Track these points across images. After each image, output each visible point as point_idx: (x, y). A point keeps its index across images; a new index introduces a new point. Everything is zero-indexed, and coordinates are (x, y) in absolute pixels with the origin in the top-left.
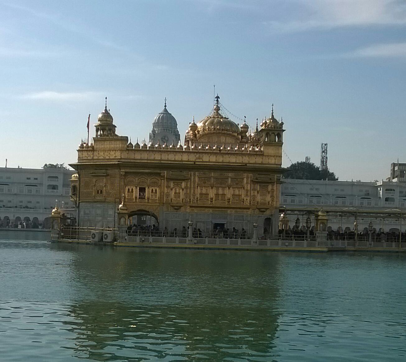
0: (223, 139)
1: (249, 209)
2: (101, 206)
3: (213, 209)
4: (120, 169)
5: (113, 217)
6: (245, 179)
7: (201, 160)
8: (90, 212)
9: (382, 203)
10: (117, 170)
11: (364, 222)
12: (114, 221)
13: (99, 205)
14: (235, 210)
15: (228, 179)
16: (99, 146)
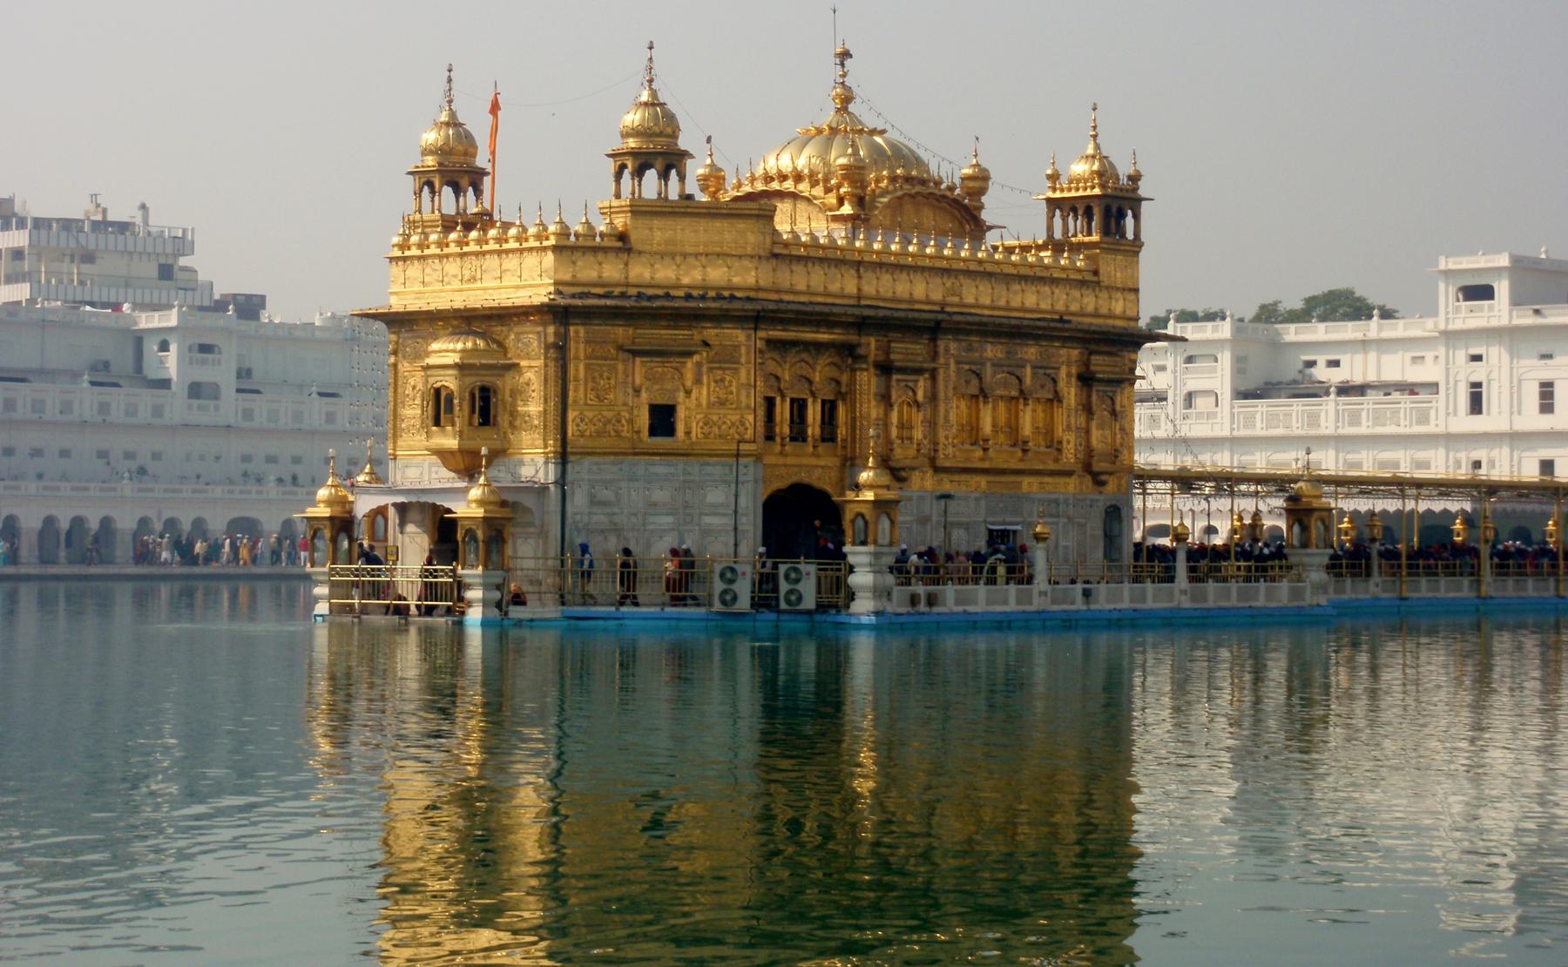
0: (928, 217)
1: (1069, 474)
2: (672, 470)
3: (991, 478)
4: (756, 329)
5: (724, 515)
6: (1063, 371)
7: (956, 299)
8: (617, 494)
9: (177, 407)
10: (739, 335)
11: (45, 488)
12: (736, 529)
13: (662, 470)
14: (1040, 479)
15: (1023, 367)
16: (659, 233)
